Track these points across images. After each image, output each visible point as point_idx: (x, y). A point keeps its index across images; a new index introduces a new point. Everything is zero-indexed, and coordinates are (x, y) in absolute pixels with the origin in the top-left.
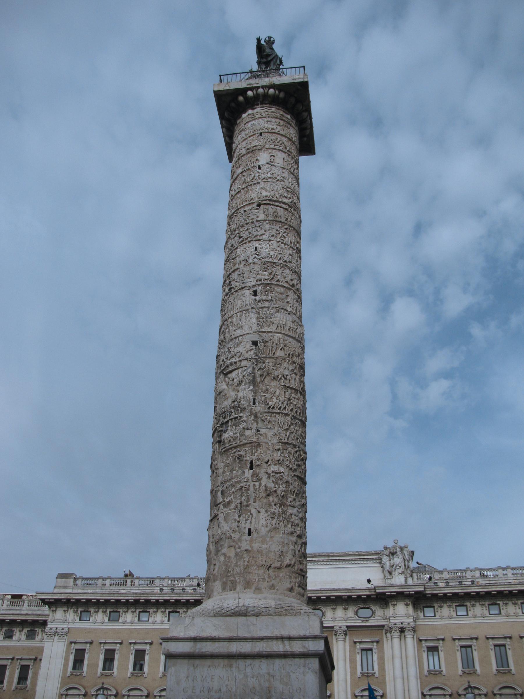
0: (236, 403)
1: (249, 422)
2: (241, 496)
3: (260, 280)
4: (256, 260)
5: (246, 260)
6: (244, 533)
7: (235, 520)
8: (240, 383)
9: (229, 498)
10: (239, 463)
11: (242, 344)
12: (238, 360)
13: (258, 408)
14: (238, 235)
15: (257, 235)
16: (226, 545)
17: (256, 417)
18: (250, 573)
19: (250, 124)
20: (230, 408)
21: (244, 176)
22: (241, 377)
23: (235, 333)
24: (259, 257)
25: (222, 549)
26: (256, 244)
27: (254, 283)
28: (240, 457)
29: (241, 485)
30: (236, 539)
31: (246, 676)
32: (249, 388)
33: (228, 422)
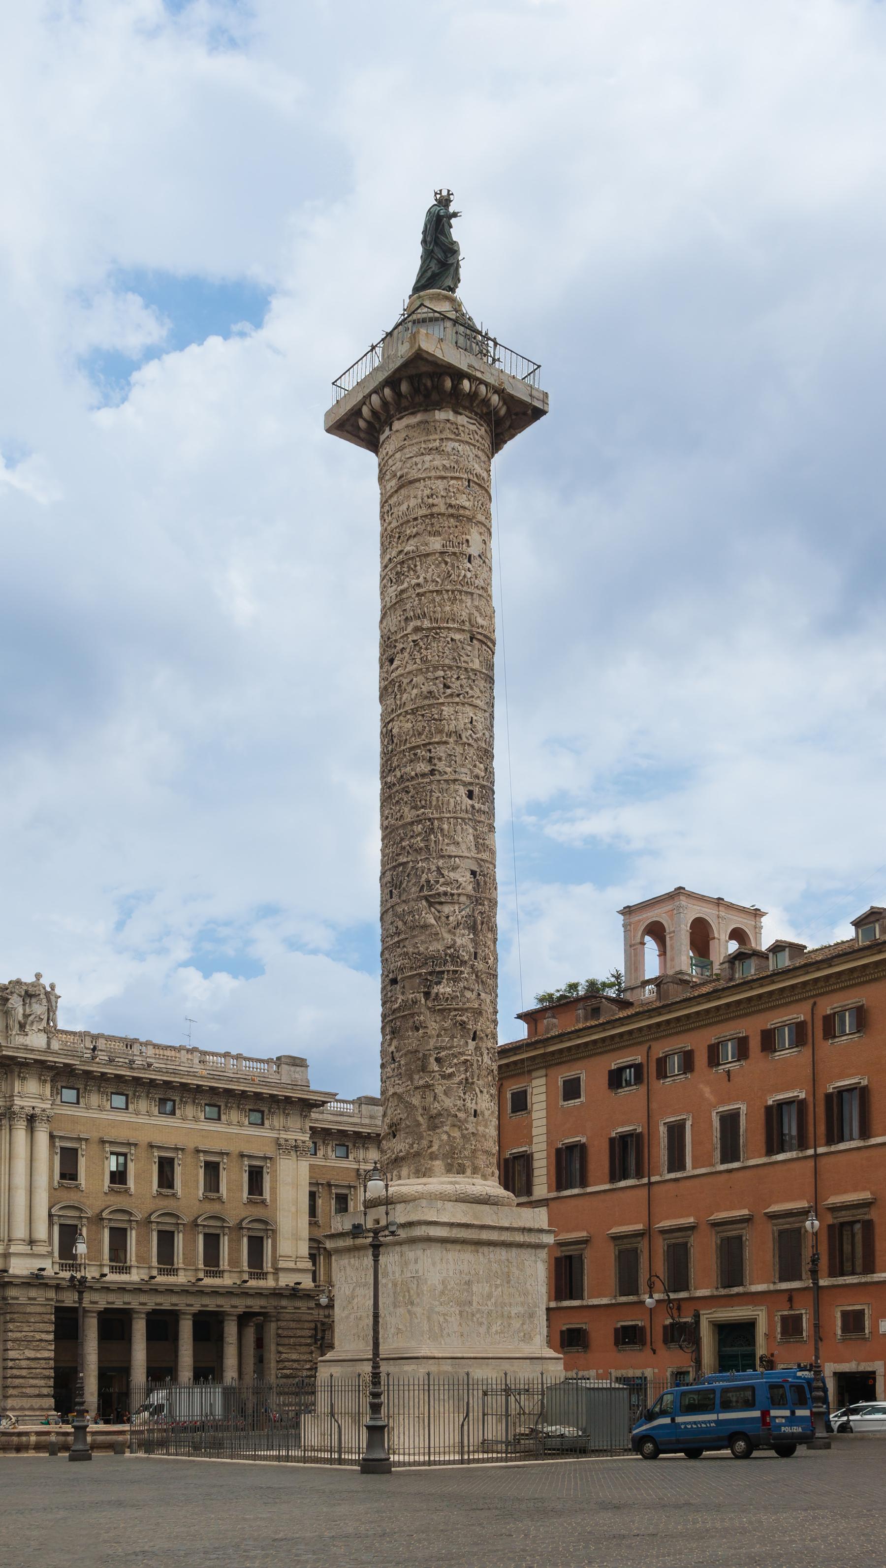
0: (452, 950)
1: (471, 981)
2: (466, 1071)
3: (477, 777)
4: (471, 741)
5: (460, 735)
6: (471, 1114)
7: (460, 1097)
8: (458, 924)
9: (450, 1070)
10: (460, 1030)
11: (459, 870)
12: (455, 891)
13: (480, 966)
14: (442, 679)
15: (473, 697)
16: (449, 1123)
17: (477, 976)
18: (477, 1158)
19: (449, 446)
20: (446, 955)
21: (446, 563)
22: (459, 917)
23: (448, 848)
24: (474, 736)
25: (443, 1126)
26: (470, 712)
27: (468, 779)
28: (463, 1024)
29: (466, 1058)
30: (462, 1119)
31: (490, 1261)
32: (469, 935)
33: (443, 972)
